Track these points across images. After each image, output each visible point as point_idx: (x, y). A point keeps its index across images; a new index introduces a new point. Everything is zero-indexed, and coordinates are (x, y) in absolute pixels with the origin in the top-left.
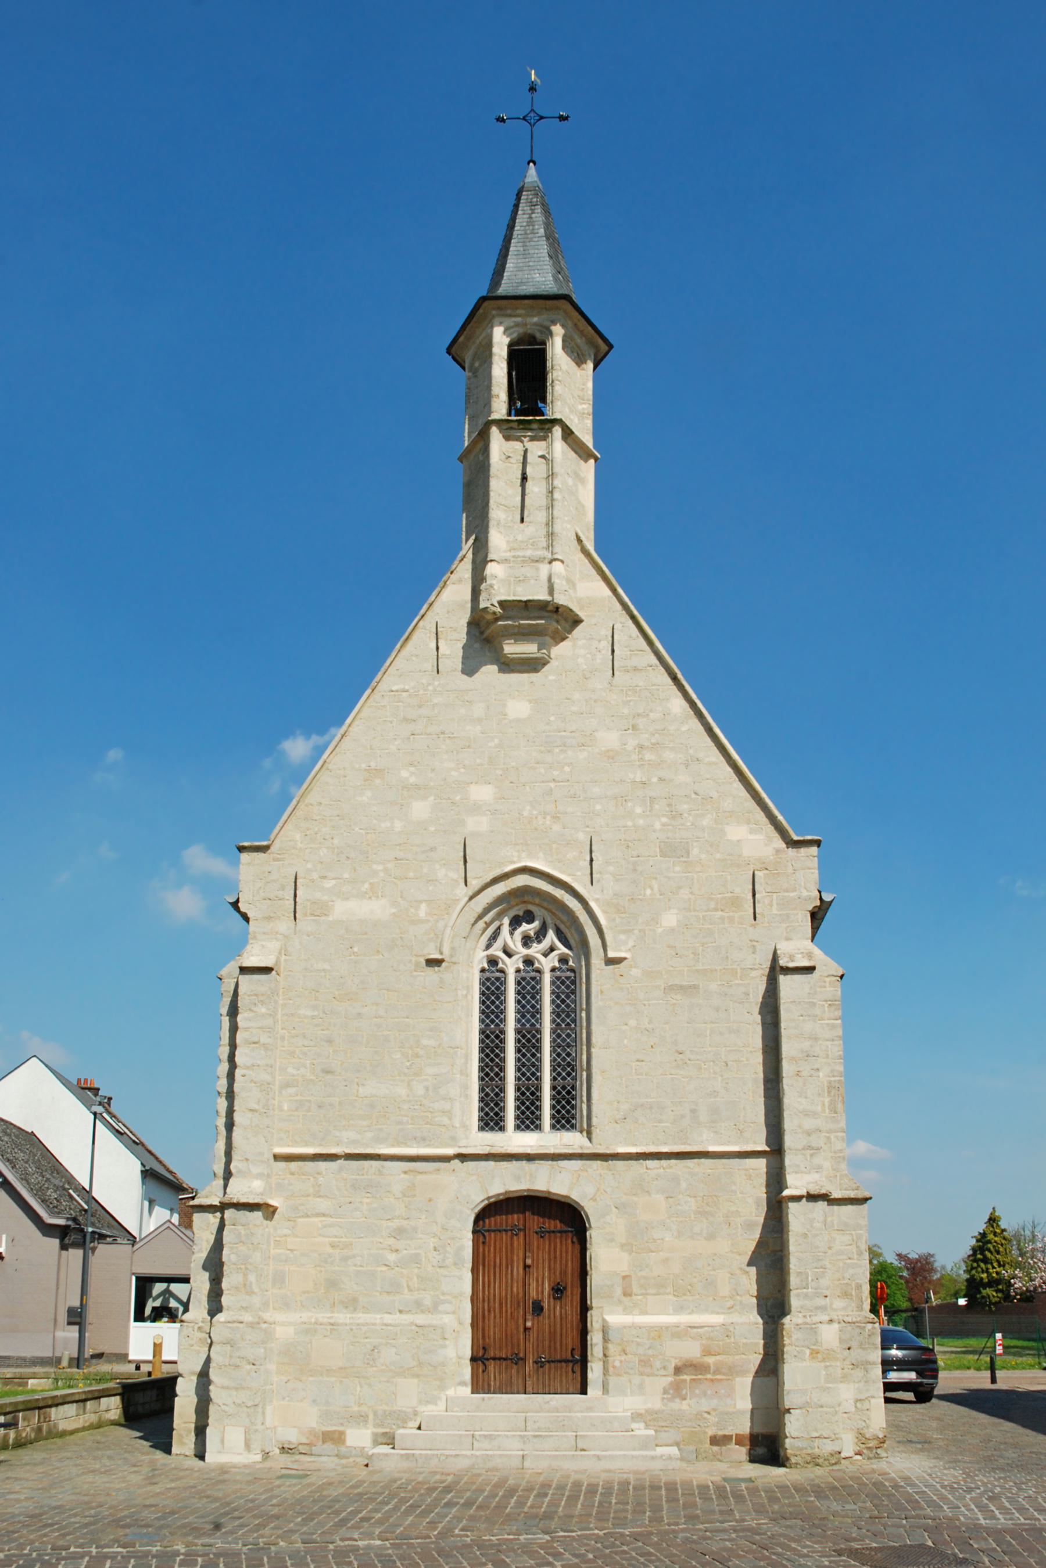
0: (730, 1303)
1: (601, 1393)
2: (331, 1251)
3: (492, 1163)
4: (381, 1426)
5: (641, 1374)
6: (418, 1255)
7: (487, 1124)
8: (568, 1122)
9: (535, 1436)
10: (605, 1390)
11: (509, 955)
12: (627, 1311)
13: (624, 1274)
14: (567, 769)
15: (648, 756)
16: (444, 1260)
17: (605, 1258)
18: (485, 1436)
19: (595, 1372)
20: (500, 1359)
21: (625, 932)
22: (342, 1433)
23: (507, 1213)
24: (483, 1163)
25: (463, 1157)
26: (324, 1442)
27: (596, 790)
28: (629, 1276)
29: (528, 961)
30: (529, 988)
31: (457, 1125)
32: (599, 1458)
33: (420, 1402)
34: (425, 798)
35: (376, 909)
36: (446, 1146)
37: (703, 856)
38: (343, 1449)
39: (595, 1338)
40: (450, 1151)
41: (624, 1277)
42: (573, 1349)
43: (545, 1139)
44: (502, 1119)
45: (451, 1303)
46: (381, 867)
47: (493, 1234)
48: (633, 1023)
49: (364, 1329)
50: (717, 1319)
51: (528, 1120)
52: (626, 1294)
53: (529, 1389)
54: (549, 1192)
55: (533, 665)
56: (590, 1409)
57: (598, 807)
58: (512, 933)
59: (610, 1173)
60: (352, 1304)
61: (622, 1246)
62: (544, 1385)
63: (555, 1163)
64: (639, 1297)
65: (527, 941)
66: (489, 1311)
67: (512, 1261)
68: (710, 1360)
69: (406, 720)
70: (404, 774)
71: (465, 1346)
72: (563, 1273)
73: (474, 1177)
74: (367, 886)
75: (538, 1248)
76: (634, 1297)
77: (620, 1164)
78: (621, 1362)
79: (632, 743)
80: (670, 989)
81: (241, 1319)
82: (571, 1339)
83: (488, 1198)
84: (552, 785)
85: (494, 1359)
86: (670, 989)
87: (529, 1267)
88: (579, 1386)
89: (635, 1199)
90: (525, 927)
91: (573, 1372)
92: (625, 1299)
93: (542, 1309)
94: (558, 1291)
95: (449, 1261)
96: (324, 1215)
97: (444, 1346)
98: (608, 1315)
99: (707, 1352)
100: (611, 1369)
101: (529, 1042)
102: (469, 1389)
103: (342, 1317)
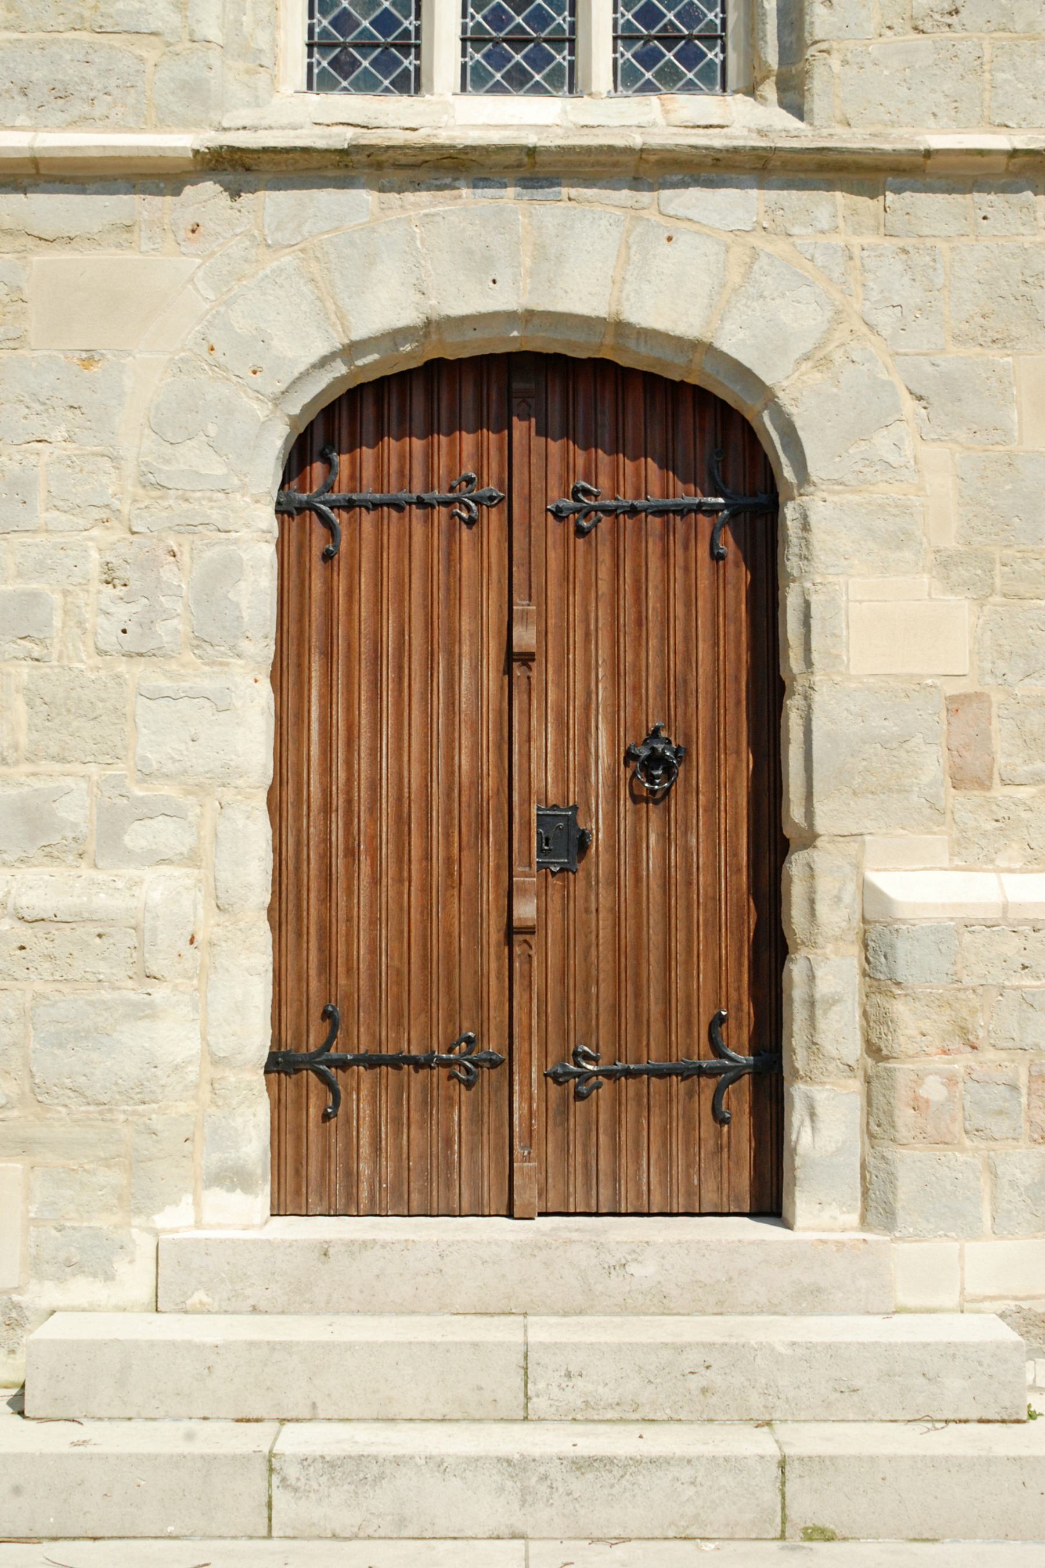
1: (854, 1218)
3: (365, 198)
6: (34, 595)
8: (691, 57)
9: (581, 1465)
10: (876, 1204)
12: (969, 851)
13: (953, 688)
16: (147, 625)
17: (874, 615)
19: (823, 1123)
20: (396, 1062)
23: (429, 431)
24: (325, 200)
25: (237, 168)
28: (979, 697)
31: (213, 33)
33: (34, 1265)
36: (161, 125)
39: (825, 975)
40: (182, 141)
41: (956, 705)
42: (718, 1021)
44: (410, 44)
45: (174, 813)
47: (368, 519)
53: (526, 1195)
54: (621, 327)
56: (811, 1298)
59: (890, 244)
61: (945, 564)
62: (591, 1177)
63: (645, 197)
64: (1023, 793)
66: (351, 853)
67: (453, 636)
71: (240, 1003)
72: (675, 688)
73: (287, 259)
75: (566, 577)
76: (999, 792)
77: (930, 209)
78: (951, 1081)
82: (715, 978)
83: (351, 350)
85: (373, 1062)
87: (527, 659)
88: (744, 1180)
89: (998, 357)
91: (720, 1119)
92: (952, 798)
93: (582, 844)
94: (654, 767)
95: (169, 631)
97: (146, 1012)
98: (889, 867)
100: (905, 1116)
102: (262, 1199)
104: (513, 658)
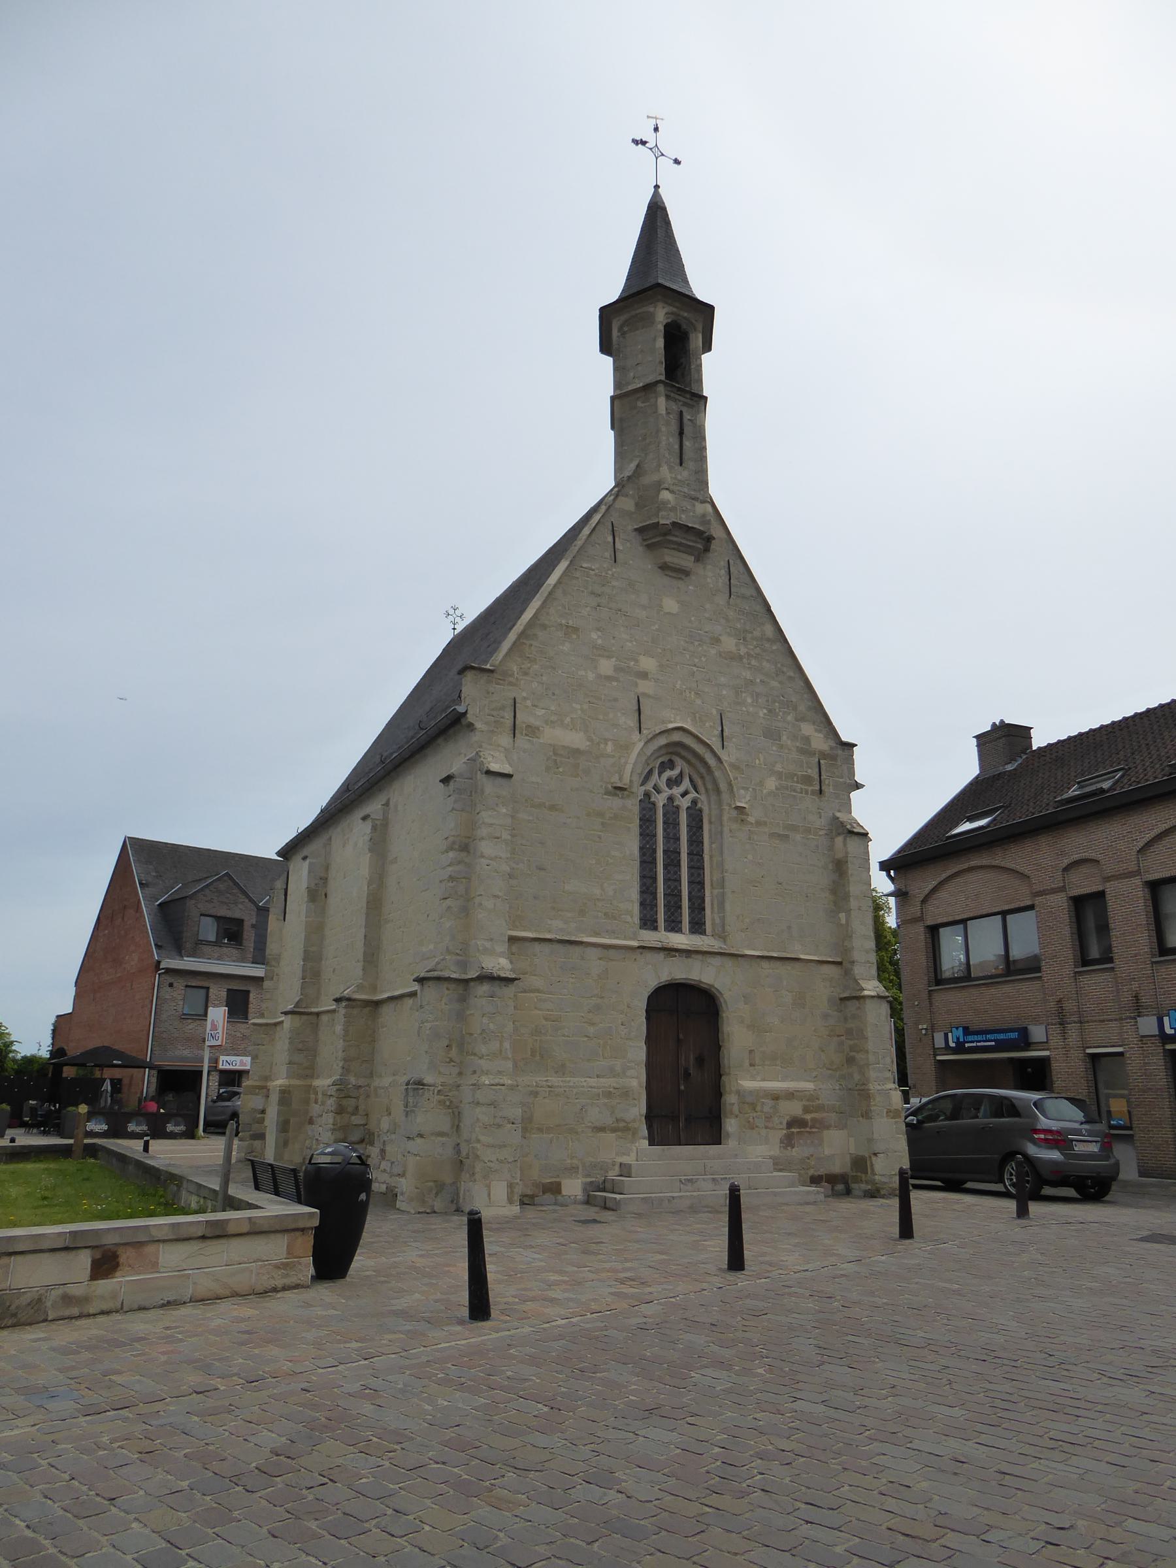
0: (815, 1074)
2: (544, 1022)
4: (588, 1176)
5: (766, 1128)
7: (645, 924)
11: (659, 792)
12: (753, 1078)
14: (703, 659)
15: (754, 662)
17: (737, 1036)
18: (689, 1180)
19: (730, 1125)
21: (743, 788)
22: (559, 1184)
26: (544, 1193)
27: (723, 680)
29: (671, 799)
30: (671, 823)
32: (775, 1194)
33: (617, 1154)
34: (609, 657)
35: (576, 739)
37: (789, 742)
38: (559, 1197)
41: (751, 1052)
43: (680, 940)
46: (578, 707)
48: (750, 857)
49: (575, 1091)
50: (810, 1086)
51: (674, 925)
52: (751, 1065)
55: (682, 573)
57: (724, 692)
58: (660, 774)
60: (561, 1070)
65: (671, 783)
68: (808, 1117)
69: (592, 593)
70: (594, 636)
74: (568, 719)
79: (743, 651)
80: (773, 835)
81: (502, 1082)
84: (695, 669)
86: (773, 835)
90: (668, 773)
94: (700, 1061)
96: (538, 991)
99: (806, 1110)
101: (672, 862)
103: (555, 1080)
104: (679, 1040)
